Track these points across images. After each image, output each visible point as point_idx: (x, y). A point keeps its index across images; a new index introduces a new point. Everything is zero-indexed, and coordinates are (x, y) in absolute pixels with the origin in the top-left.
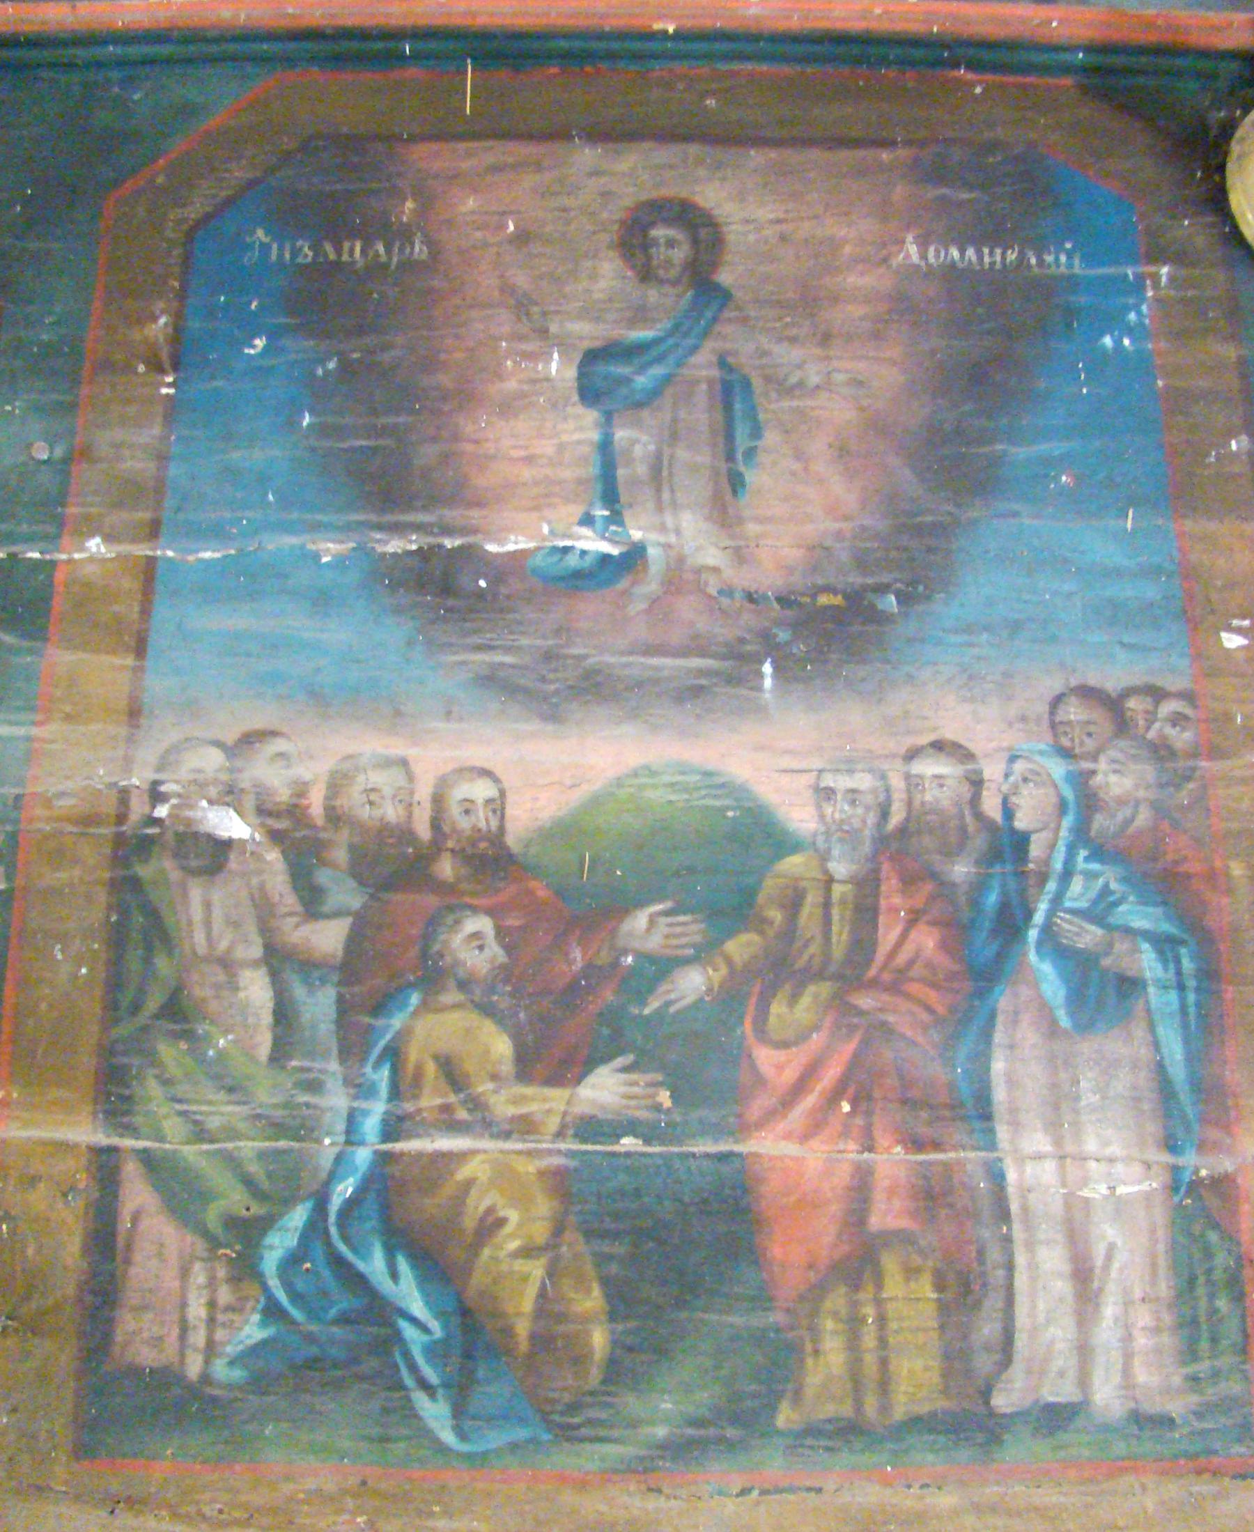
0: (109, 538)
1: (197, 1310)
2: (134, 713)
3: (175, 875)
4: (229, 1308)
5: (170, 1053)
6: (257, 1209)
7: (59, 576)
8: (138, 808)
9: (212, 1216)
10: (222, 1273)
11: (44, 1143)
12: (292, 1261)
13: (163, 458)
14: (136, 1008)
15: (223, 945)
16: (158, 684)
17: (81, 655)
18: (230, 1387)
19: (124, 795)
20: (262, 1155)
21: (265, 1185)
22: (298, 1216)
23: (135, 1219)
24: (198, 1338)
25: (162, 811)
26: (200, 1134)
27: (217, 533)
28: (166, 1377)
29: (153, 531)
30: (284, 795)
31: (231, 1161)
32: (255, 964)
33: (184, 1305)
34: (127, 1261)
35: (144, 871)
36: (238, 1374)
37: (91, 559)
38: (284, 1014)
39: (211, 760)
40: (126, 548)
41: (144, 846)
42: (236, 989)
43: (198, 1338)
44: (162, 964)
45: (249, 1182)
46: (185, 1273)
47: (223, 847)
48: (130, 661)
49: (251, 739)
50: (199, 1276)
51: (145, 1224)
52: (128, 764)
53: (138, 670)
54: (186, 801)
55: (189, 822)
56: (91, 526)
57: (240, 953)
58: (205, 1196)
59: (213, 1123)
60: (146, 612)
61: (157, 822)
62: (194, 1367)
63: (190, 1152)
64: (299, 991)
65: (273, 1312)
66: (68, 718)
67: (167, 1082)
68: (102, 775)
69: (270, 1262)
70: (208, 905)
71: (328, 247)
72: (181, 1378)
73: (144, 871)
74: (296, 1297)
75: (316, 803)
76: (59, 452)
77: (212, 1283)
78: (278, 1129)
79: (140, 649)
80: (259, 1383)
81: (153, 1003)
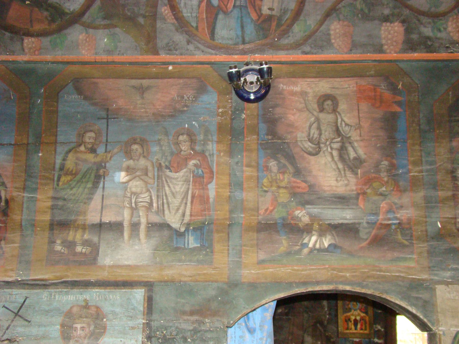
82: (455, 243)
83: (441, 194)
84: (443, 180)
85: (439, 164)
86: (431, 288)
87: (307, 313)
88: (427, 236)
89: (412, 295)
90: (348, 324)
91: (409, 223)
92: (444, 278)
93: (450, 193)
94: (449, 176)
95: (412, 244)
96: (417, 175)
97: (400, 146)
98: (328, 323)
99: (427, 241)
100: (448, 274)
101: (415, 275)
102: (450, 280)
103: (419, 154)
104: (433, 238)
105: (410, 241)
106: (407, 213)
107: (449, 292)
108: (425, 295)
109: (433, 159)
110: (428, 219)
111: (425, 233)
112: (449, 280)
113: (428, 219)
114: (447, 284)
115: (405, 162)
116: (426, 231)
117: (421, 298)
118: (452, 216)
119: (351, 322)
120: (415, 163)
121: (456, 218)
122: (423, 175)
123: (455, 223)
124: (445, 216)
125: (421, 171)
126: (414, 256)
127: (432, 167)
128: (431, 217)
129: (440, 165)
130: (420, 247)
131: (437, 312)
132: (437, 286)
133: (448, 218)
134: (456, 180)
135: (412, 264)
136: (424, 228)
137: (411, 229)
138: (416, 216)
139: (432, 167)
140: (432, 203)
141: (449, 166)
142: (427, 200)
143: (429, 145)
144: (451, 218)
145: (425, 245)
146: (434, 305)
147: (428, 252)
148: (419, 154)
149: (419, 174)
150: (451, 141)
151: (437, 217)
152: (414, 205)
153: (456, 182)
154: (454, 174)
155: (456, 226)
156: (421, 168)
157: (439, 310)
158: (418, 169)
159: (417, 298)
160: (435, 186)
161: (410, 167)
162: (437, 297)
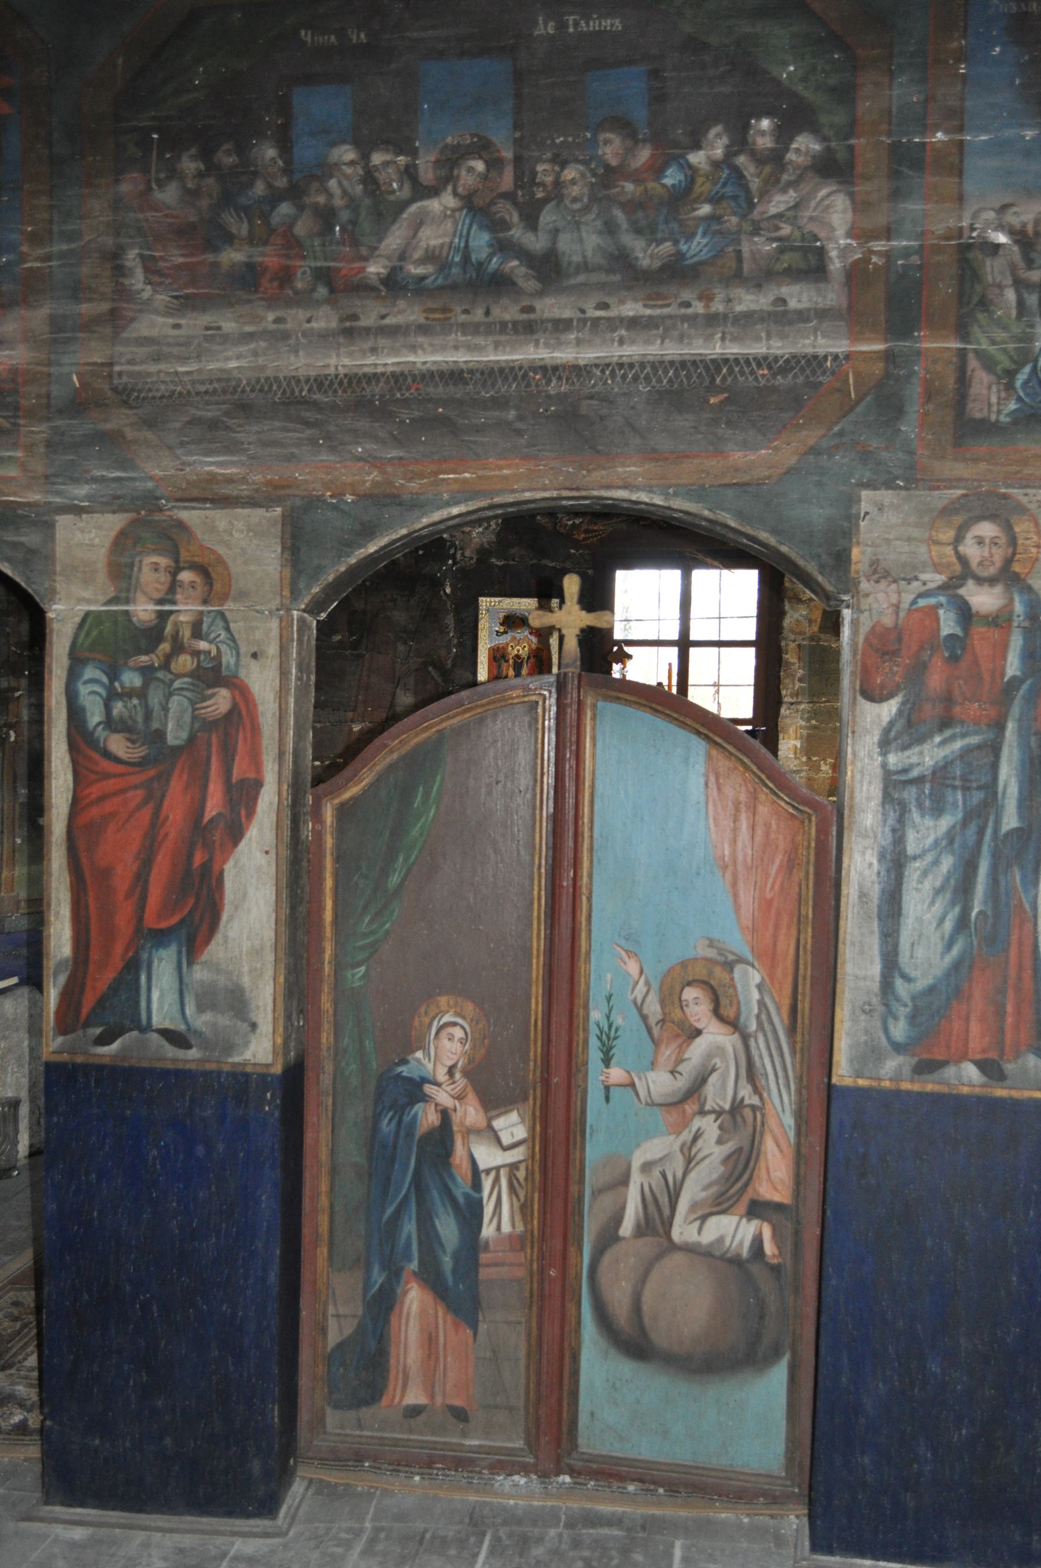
0: (946, 132)
1: (994, 399)
2: (961, 199)
3: (980, 257)
4: (1005, 399)
5: (981, 317)
6: (1013, 367)
7: (928, 148)
8: (966, 233)
9: (999, 368)
10: (1002, 387)
11: (940, 348)
12: (1026, 383)
13: (963, 99)
14: (969, 303)
15: (998, 280)
16: (969, 187)
17: (937, 178)
18: (1007, 423)
19: (961, 229)
20: (1015, 349)
21: (1016, 358)
22: (1027, 369)
23: (973, 371)
24: (995, 408)
25: (975, 234)
26: (993, 342)
27: (985, 130)
28: (984, 421)
29: (961, 129)
30: (1018, 227)
31: (1005, 351)
32: (1010, 286)
33: (989, 399)
34: (970, 386)
35: (970, 255)
36: (1008, 419)
37: (939, 141)
38: (1021, 303)
39: (991, 215)
40: (952, 136)
41: (969, 247)
42: (1003, 295)
43: (995, 408)
44: (978, 288)
45: (1011, 358)
46: (989, 388)
47: (997, 247)
48: (956, 180)
49: (1005, 208)
50: (994, 389)
51: (976, 373)
52: (960, 219)
53: (961, 184)
54: (984, 230)
55: (984, 238)
56: (937, 128)
57: (1004, 283)
58: (996, 363)
59: (999, 339)
60: (961, 161)
61: (973, 238)
62: (993, 417)
63: (992, 349)
64: (1026, 295)
65: (1019, 399)
66: (937, 202)
67: (980, 327)
68: (952, 223)
69: (1018, 383)
70: (992, 267)
71: (1023, 5)
72: (989, 421)
73: (970, 255)
74: (1027, 395)
75: (1030, 229)
76: (922, 98)
77: (999, 391)
78: (1020, 340)
79: (960, 174)
80: (1015, 422)
81: (975, 299)
82: (106, 421)
83: (86, 309)
84: (96, 276)
85: (87, 238)
86: (46, 522)
87: (405, 643)
88: (48, 406)
89: (5, 538)
90: (499, 667)
91: (13, 380)
92: (75, 499)
93: (104, 307)
94: (108, 266)
95: (15, 424)
96: (38, 268)
97: (6, 198)
98: (454, 665)
99: (48, 419)
100: (82, 491)
101: (15, 494)
102: (87, 504)
103: (45, 216)
104: (60, 412)
105: (13, 420)
106: (10, 357)
107: (82, 531)
108: (30, 538)
109: (76, 227)
110: (52, 370)
111: (45, 401)
112: (82, 504)
113: (52, 370)
114: (78, 511)
115: (14, 236)
116: (48, 396)
117: (22, 544)
118: (104, 361)
119: (507, 661)
120: (35, 239)
121: (111, 364)
122: (50, 267)
123: (110, 376)
124: (91, 361)
125: (48, 258)
126: (19, 454)
127: (73, 246)
128: (59, 365)
129: (90, 241)
130: (33, 432)
131: (55, 573)
132: (57, 518)
133: (95, 364)
134: (124, 275)
135: (13, 472)
136: (43, 391)
137: (15, 392)
138: (28, 364)
139: (73, 246)
140: (65, 332)
141: (109, 241)
142: (56, 324)
143: (70, 193)
144: (102, 364)
145: (43, 427)
146: (50, 558)
147: (49, 444)
148: (45, 216)
149: (43, 265)
150: (117, 181)
151: (72, 364)
152: (29, 338)
153: (121, 280)
154: (119, 262)
155: (111, 383)
156: (47, 250)
157: (58, 569)
158: (41, 252)
159: (15, 545)
160: (77, 291)
161: (24, 249)
162: (57, 542)
